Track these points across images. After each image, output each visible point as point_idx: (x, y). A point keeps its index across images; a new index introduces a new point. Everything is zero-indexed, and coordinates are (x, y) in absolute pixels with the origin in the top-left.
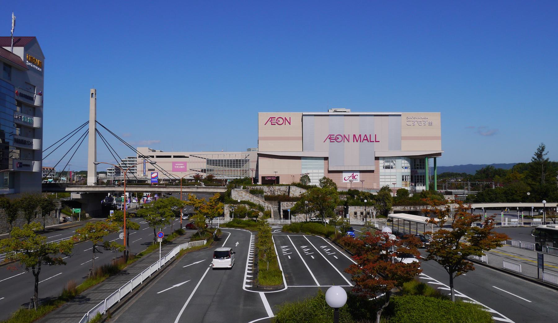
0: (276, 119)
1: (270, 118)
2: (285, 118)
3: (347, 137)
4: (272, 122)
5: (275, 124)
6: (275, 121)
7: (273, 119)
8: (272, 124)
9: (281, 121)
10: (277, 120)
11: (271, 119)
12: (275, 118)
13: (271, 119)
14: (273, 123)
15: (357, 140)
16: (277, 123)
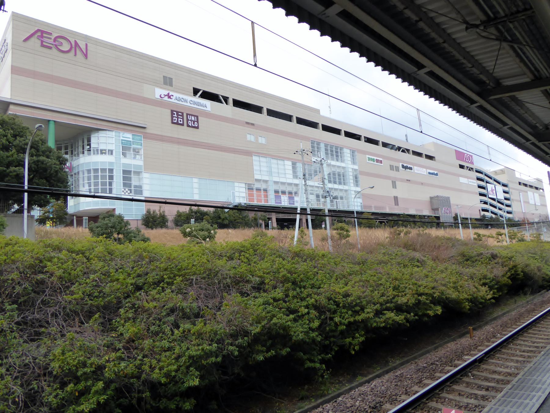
0: (53, 37)
1: (38, 31)
2: (76, 42)
3: (83, 47)
4: (42, 42)
5: (50, 48)
6: (52, 41)
7: (44, 35)
8: (42, 45)
9: (66, 47)
10: (55, 40)
11: (39, 34)
12: (51, 34)
13: (39, 34)
14: (44, 44)
15: (85, 52)
16: (56, 46)
